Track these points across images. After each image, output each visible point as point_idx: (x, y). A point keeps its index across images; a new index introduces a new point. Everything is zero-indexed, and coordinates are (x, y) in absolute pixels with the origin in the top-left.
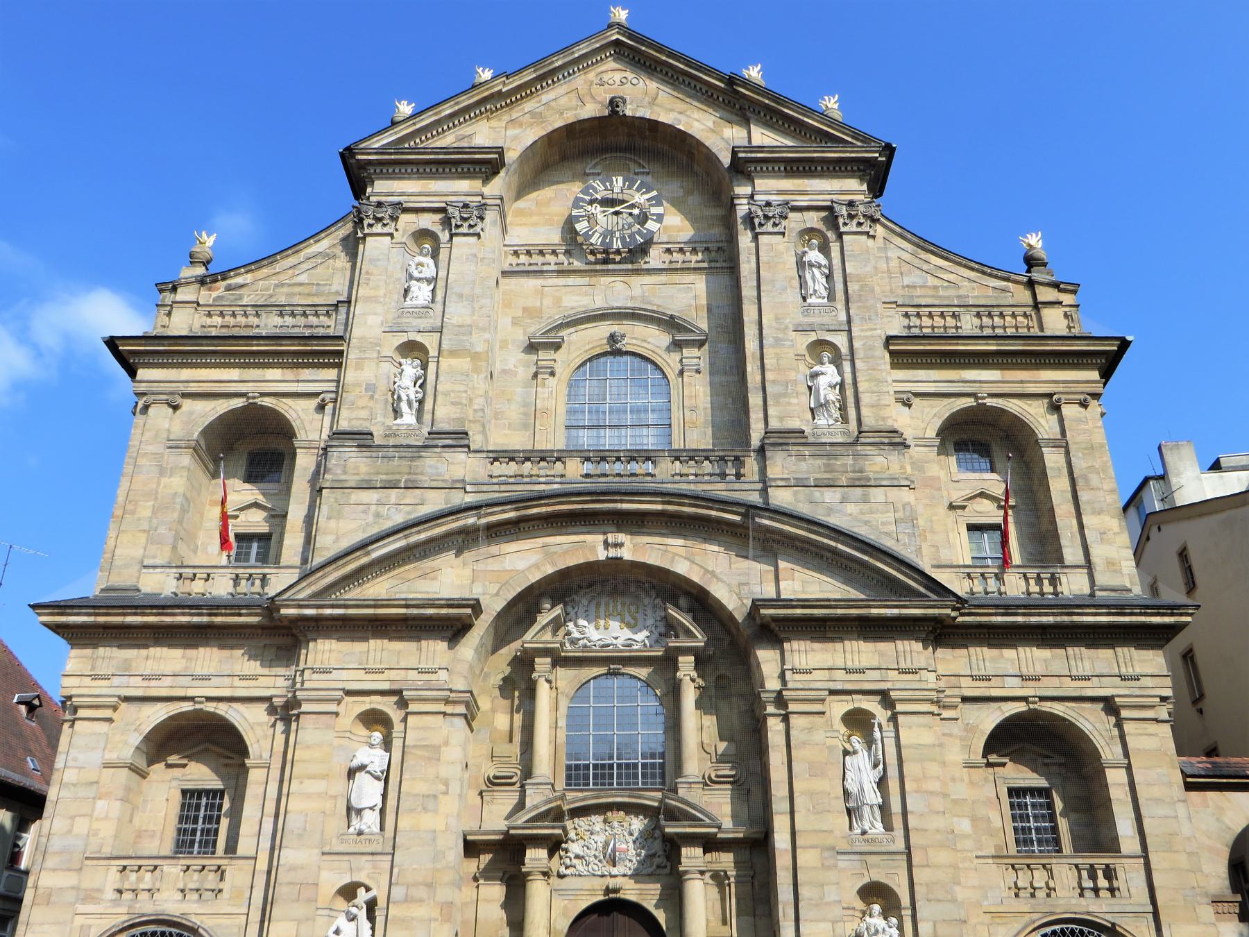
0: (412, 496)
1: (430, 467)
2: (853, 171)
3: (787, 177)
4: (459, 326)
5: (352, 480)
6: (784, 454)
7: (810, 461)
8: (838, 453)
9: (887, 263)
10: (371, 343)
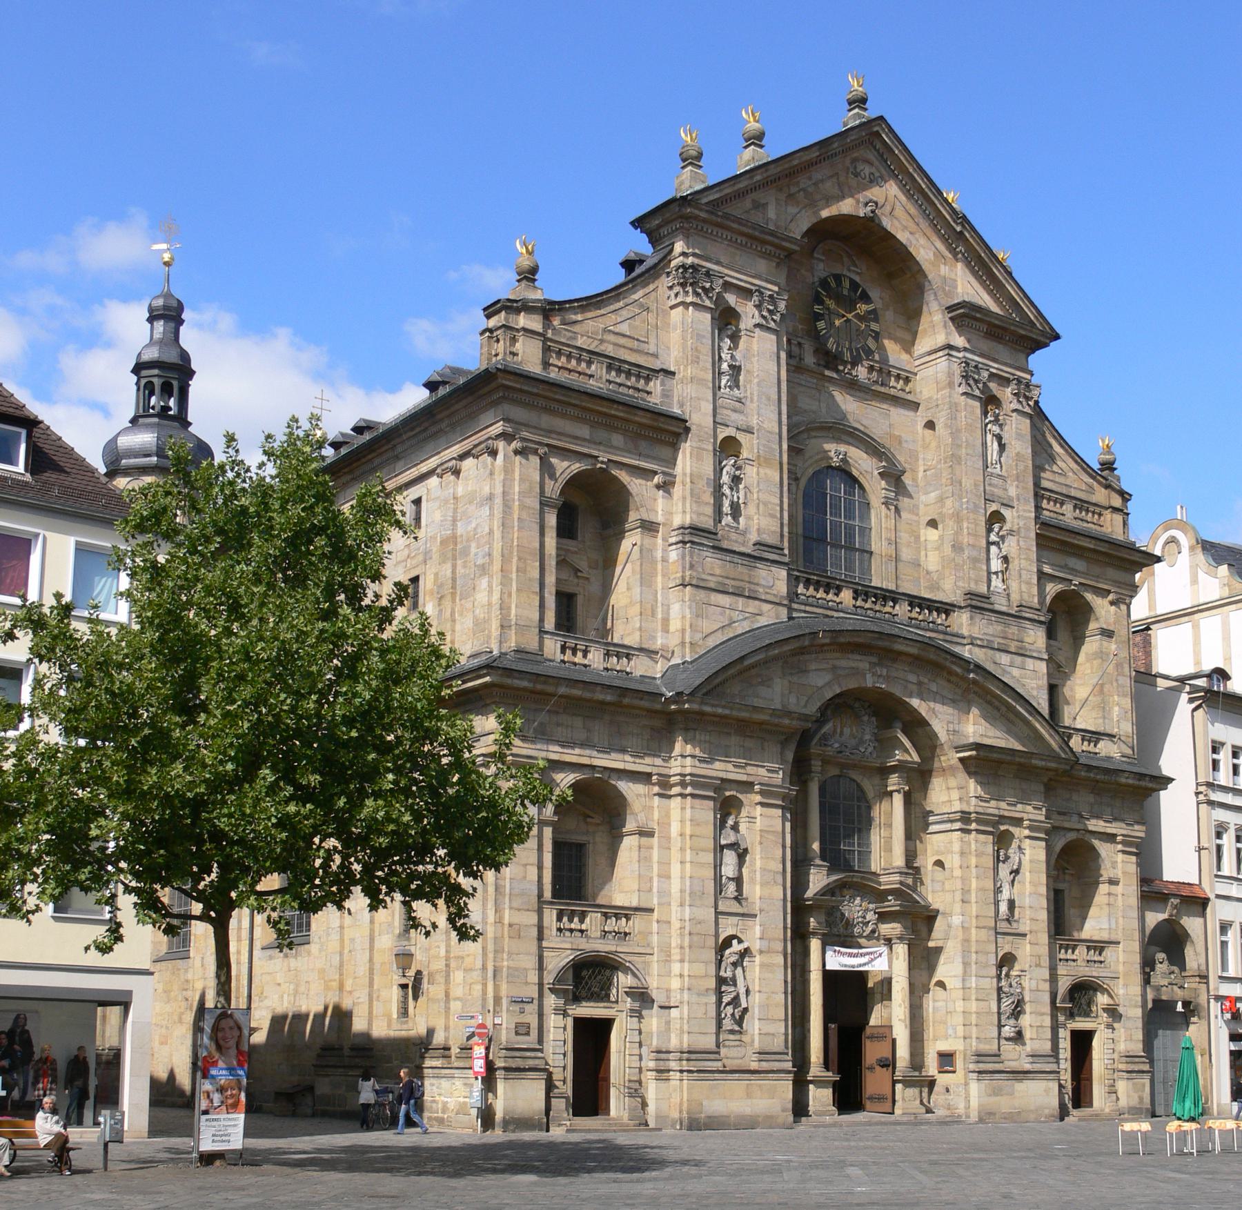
0: (753, 606)
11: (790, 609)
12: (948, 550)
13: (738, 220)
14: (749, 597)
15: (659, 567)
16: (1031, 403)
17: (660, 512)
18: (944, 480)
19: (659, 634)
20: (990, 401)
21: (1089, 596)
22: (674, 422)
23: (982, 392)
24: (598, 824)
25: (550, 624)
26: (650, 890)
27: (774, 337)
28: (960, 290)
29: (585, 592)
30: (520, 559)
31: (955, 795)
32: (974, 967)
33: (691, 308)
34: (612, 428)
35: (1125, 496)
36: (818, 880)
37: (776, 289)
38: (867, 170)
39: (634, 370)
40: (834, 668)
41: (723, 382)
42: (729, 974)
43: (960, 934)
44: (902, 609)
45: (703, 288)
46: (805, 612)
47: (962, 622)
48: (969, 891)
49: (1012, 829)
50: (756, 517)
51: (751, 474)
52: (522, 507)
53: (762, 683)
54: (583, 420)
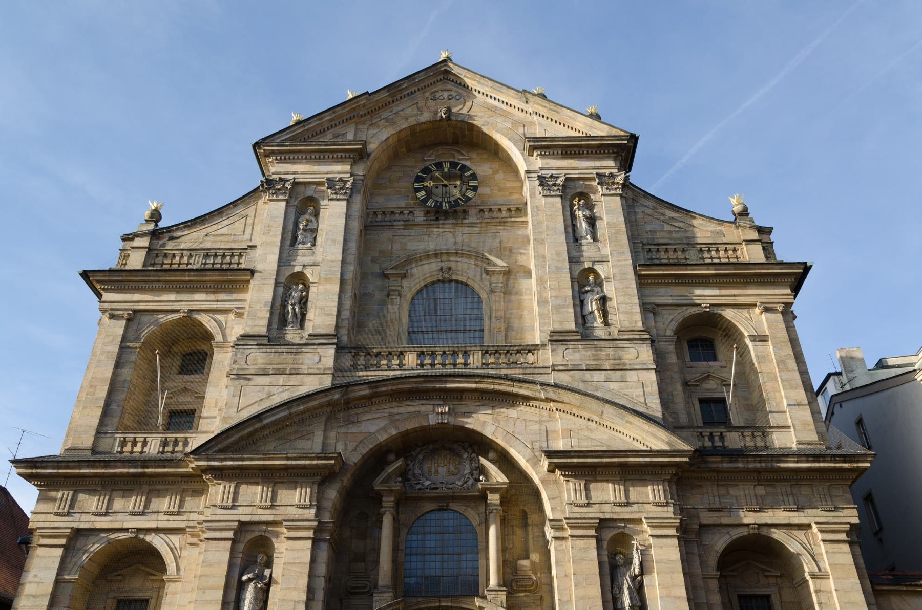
0: (294, 380)
1: (308, 359)
2: (609, 153)
3: (563, 158)
4: (332, 261)
5: (252, 369)
6: (565, 347)
7: (583, 352)
8: (603, 346)
9: (635, 216)
10: (270, 273)
38: (446, 95)
40: (391, 415)
53: (301, 437)
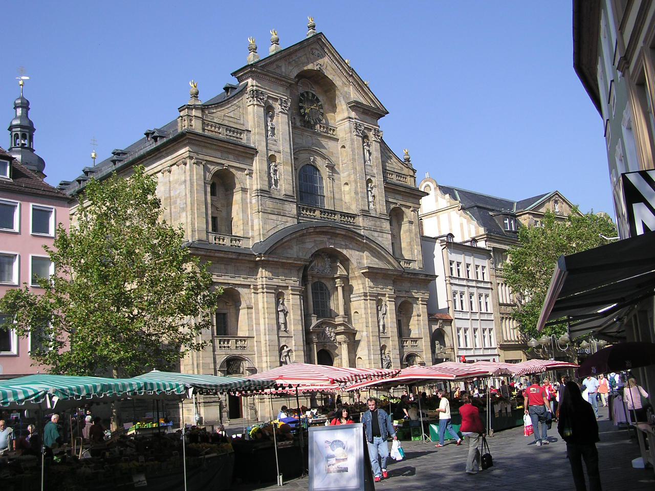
0: (284, 219)
11: (298, 219)
12: (353, 194)
13: (272, 73)
14: (283, 216)
15: (249, 205)
16: (380, 138)
17: (248, 185)
18: (350, 168)
19: (250, 231)
20: (365, 137)
21: (403, 209)
22: (252, 150)
23: (362, 134)
24: (231, 306)
25: (210, 229)
26: (253, 330)
27: (287, 116)
28: (352, 96)
29: (221, 215)
30: (198, 205)
31: (361, 286)
32: (372, 351)
33: (256, 106)
34: (230, 153)
35: (414, 171)
36: (314, 322)
37: (286, 98)
39: (236, 130)
40: (315, 241)
41: (269, 134)
42: (284, 360)
43: (366, 339)
44: (337, 217)
45: (260, 99)
46: (303, 220)
47: (360, 221)
48: (368, 323)
49: (382, 298)
50: (283, 185)
51: (281, 168)
52: (197, 185)
53: (289, 248)
54: (216, 150)
